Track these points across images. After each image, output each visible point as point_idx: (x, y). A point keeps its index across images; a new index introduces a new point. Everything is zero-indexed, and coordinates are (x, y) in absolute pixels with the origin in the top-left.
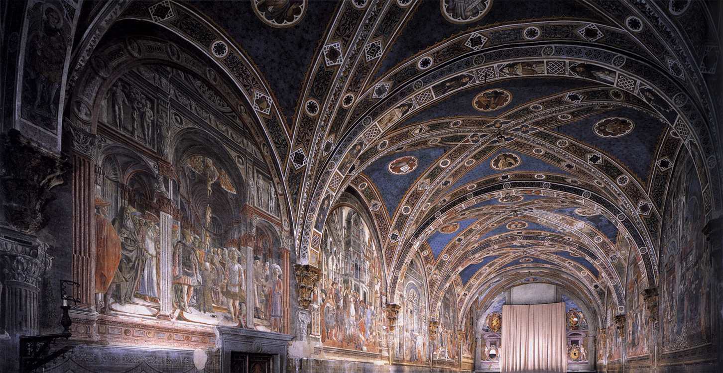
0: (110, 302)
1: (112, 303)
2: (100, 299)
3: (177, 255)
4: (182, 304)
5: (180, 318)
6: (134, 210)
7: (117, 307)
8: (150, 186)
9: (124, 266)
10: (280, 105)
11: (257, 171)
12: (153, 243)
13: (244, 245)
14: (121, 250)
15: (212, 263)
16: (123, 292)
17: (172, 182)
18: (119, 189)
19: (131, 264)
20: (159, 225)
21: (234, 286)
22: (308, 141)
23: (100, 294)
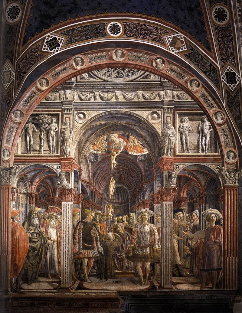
0: (21, 284)
1: (22, 284)
2: (14, 282)
3: (77, 234)
4: (82, 276)
5: (80, 287)
6: (40, 209)
7: (25, 286)
8: (53, 184)
9: (31, 254)
10: (191, 34)
11: (181, 115)
12: (55, 231)
13: (158, 203)
14: (28, 243)
15: (116, 231)
16: (30, 273)
17: (73, 173)
18: (28, 197)
19: (36, 252)
20: (60, 214)
21: (145, 247)
22: (232, 54)
23: (14, 279)
